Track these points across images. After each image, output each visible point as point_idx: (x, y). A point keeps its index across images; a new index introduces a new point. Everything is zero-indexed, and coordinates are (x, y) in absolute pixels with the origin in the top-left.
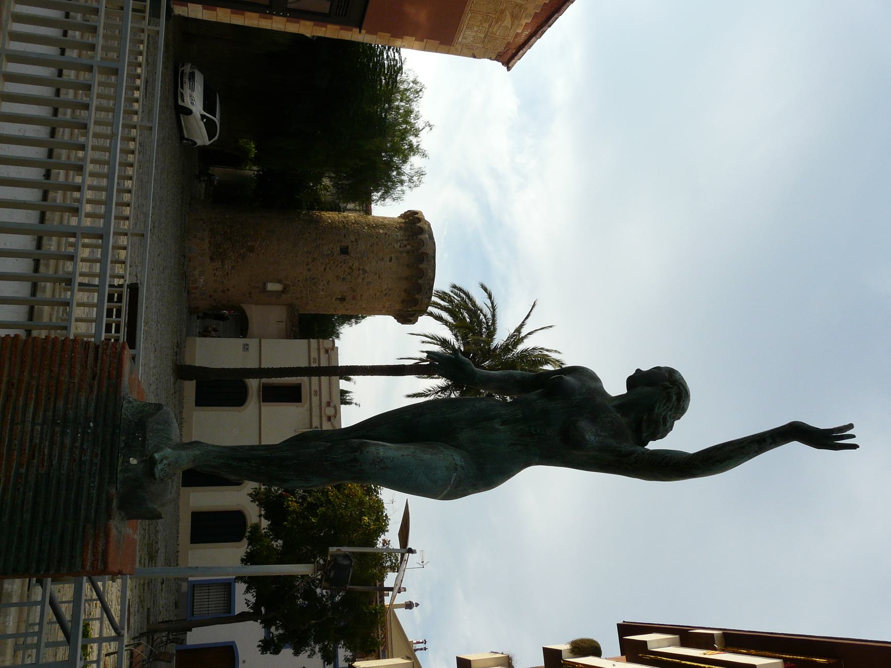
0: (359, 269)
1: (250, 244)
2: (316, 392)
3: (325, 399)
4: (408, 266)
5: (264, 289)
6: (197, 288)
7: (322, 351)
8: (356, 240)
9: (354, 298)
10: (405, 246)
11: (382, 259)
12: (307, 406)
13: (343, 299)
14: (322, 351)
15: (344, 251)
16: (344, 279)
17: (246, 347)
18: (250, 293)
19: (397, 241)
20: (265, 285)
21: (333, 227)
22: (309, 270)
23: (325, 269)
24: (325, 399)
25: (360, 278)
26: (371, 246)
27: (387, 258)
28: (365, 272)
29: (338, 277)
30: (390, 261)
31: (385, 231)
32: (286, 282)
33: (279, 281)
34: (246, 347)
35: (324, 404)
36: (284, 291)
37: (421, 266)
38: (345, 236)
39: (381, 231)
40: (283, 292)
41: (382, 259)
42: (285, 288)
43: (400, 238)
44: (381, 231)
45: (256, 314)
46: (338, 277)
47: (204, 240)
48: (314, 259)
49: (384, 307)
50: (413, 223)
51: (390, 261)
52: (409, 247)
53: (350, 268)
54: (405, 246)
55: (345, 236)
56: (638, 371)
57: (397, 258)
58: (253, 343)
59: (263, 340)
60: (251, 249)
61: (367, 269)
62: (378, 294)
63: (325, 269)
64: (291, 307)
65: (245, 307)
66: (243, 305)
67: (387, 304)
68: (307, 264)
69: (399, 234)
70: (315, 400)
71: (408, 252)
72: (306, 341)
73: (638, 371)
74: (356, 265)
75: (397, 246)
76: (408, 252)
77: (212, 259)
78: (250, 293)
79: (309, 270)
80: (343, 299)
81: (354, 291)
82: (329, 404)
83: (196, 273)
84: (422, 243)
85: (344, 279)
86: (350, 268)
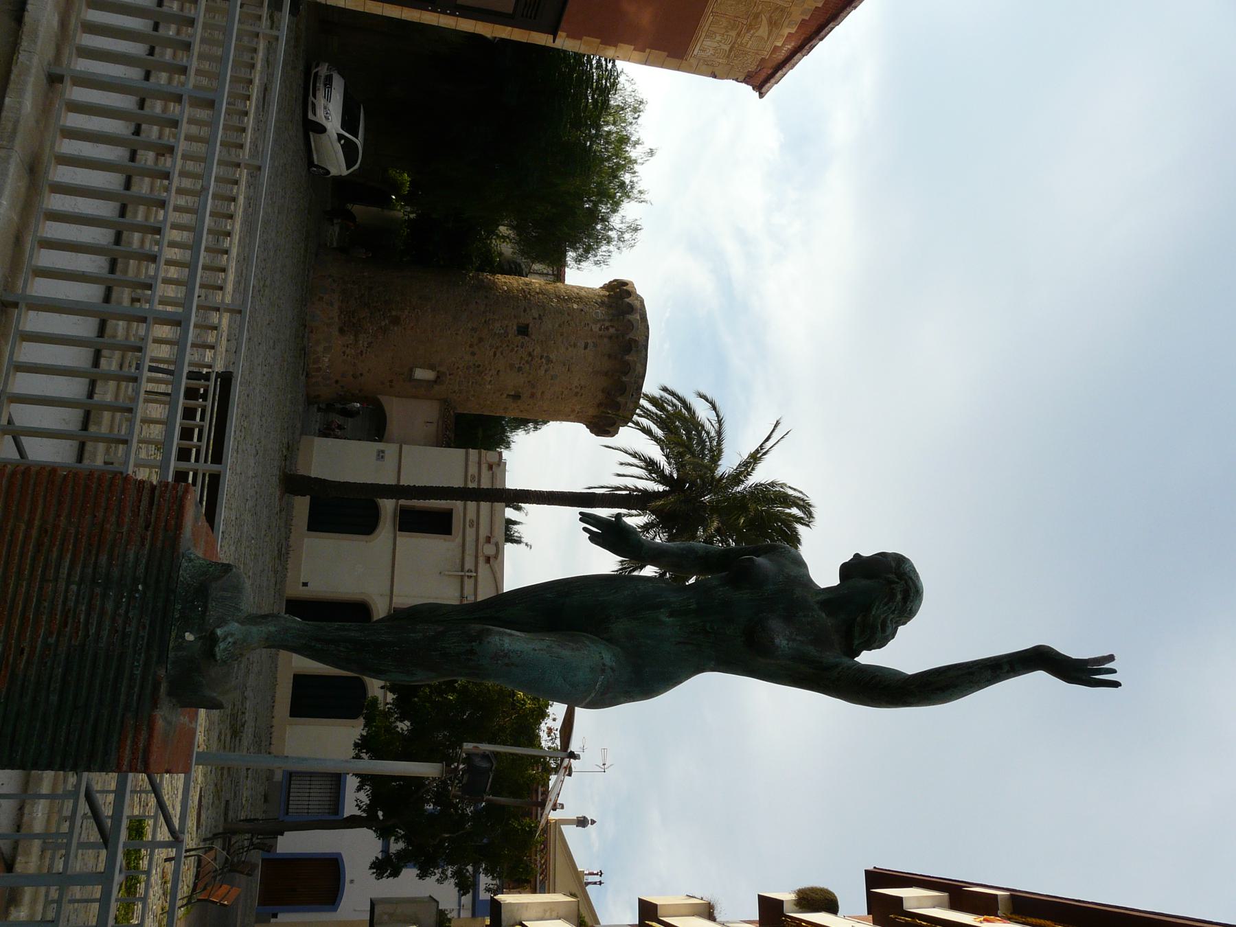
1: (394, 313)
2: (471, 522)
3: (484, 532)
4: (610, 356)
5: (410, 378)
6: (319, 369)
9: (533, 395)
10: (607, 328)
11: (575, 345)
12: (459, 540)
13: (517, 397)
15: (523, 330)
17: (381, 455)
18: (391, 381)
19: (596, 321)
20: (411, 371)
21: (509, 297)
22: (473, 354)
23: (495, 354)
24: (484, 532)
27: (581, 344)
28: (549, 361)
29: (512, 366)
30: (586, 348)
31: (581, 307)
32: (442, 369)
33: (431, 367)
34: (381, 455)
35: (482, 540)
36: (438, 380)
37: (627, 357)
38: (525, 310)
39: (575, 306)
40: (435, 382)
41: (575, 345)
42: (438, 377)
43: (600, 317)
44: (575, 306)
45: (395, 409)
46: (512, 366)
47: (332, 304)
48: (481, 340)
49: (573, 411)
50: (621, 299)
51: (586, 348)
52: (612, 330)
53: (530, 354)
54: (607, 328)
55: (525, 310)
56: (857, 556)
57: (595, 345)
58: (390, 449)
60: (396, 321)
61: (552, 356)
63: (495, 354)
64: (446, 403)
65: (384, 399)
67: (577, 408)
68: (471, 346)
69: (601, 312)
70: (470, 532)
71: (610, 338)
72: (462, 451)
73: (857, 556)
74: (538, 350)
75: (596, 328)
77: (341, 331)
78: (391, 381)
80: (517, 397)
82: (488, 540)
83: (320, 349)
84: (630, 326)
85: (520, 369)
86: (530, 354)
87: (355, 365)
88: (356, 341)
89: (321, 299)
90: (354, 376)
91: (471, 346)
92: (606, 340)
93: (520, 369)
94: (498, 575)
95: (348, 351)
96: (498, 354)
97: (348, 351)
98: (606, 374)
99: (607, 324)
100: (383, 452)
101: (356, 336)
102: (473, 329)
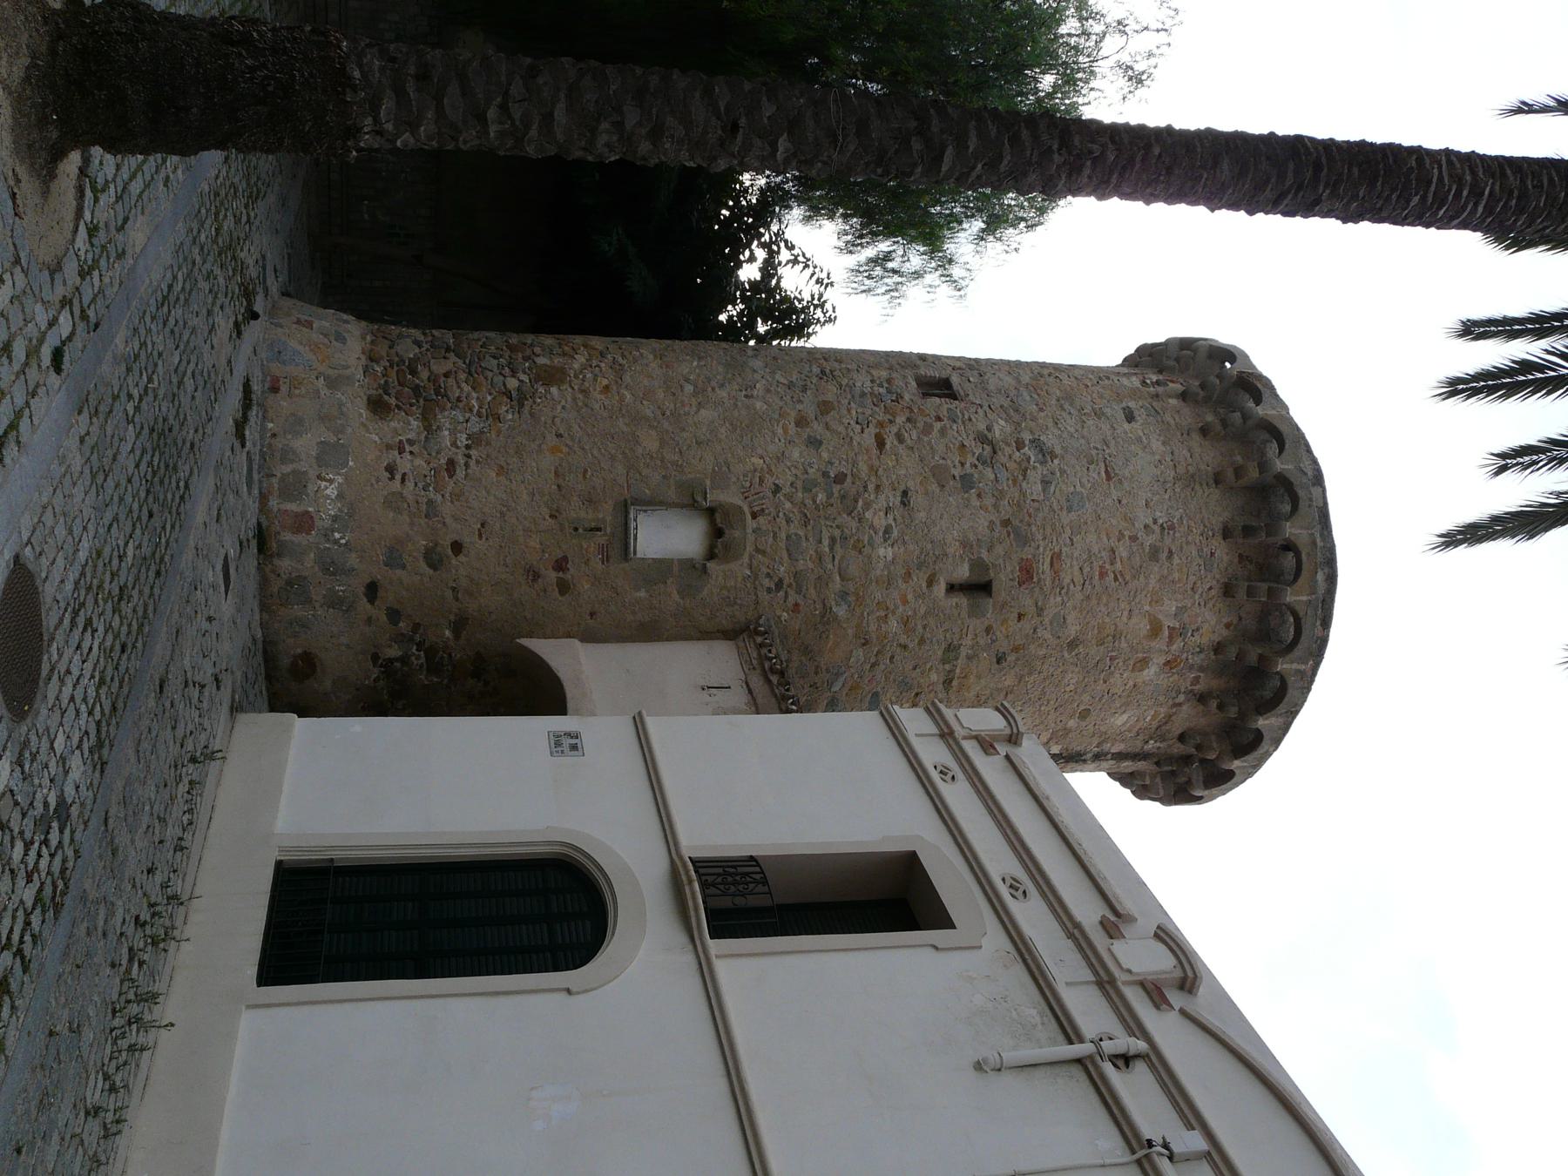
0: (1020, 445)
1: (541, 361)
4: (1204, 431)
6: (303, 523)
9: (1027, 573)
16: (967, 482)
18: (560, 565)
22: (814, 443)
23: (881, 443)
25: (1035, 476)
28: (1046, 454)
29: (940, 475)
32: (729, 497)
33: (691, 500)
40: (711, 555)
42: (717, 533)
46: (940, 475)
48: (825, 408)
49: (1155, 630)
61: (1050, 440)
62: (1122, 552)
63: (881, 443)
66: (525, 642)
74: (1001, 428)
77: (377, 406)
78: (560, 565)
80: (978, 588)
81: (1024, 540)
86: (982, 439)
87: (431, 510)
88: (430, 428)
90: (433, 559)
91: (801, 422)
93: (967, 482)
95: (405, 464)
97: (405, 464)
98: (1218, 479)
102: (790, 386)
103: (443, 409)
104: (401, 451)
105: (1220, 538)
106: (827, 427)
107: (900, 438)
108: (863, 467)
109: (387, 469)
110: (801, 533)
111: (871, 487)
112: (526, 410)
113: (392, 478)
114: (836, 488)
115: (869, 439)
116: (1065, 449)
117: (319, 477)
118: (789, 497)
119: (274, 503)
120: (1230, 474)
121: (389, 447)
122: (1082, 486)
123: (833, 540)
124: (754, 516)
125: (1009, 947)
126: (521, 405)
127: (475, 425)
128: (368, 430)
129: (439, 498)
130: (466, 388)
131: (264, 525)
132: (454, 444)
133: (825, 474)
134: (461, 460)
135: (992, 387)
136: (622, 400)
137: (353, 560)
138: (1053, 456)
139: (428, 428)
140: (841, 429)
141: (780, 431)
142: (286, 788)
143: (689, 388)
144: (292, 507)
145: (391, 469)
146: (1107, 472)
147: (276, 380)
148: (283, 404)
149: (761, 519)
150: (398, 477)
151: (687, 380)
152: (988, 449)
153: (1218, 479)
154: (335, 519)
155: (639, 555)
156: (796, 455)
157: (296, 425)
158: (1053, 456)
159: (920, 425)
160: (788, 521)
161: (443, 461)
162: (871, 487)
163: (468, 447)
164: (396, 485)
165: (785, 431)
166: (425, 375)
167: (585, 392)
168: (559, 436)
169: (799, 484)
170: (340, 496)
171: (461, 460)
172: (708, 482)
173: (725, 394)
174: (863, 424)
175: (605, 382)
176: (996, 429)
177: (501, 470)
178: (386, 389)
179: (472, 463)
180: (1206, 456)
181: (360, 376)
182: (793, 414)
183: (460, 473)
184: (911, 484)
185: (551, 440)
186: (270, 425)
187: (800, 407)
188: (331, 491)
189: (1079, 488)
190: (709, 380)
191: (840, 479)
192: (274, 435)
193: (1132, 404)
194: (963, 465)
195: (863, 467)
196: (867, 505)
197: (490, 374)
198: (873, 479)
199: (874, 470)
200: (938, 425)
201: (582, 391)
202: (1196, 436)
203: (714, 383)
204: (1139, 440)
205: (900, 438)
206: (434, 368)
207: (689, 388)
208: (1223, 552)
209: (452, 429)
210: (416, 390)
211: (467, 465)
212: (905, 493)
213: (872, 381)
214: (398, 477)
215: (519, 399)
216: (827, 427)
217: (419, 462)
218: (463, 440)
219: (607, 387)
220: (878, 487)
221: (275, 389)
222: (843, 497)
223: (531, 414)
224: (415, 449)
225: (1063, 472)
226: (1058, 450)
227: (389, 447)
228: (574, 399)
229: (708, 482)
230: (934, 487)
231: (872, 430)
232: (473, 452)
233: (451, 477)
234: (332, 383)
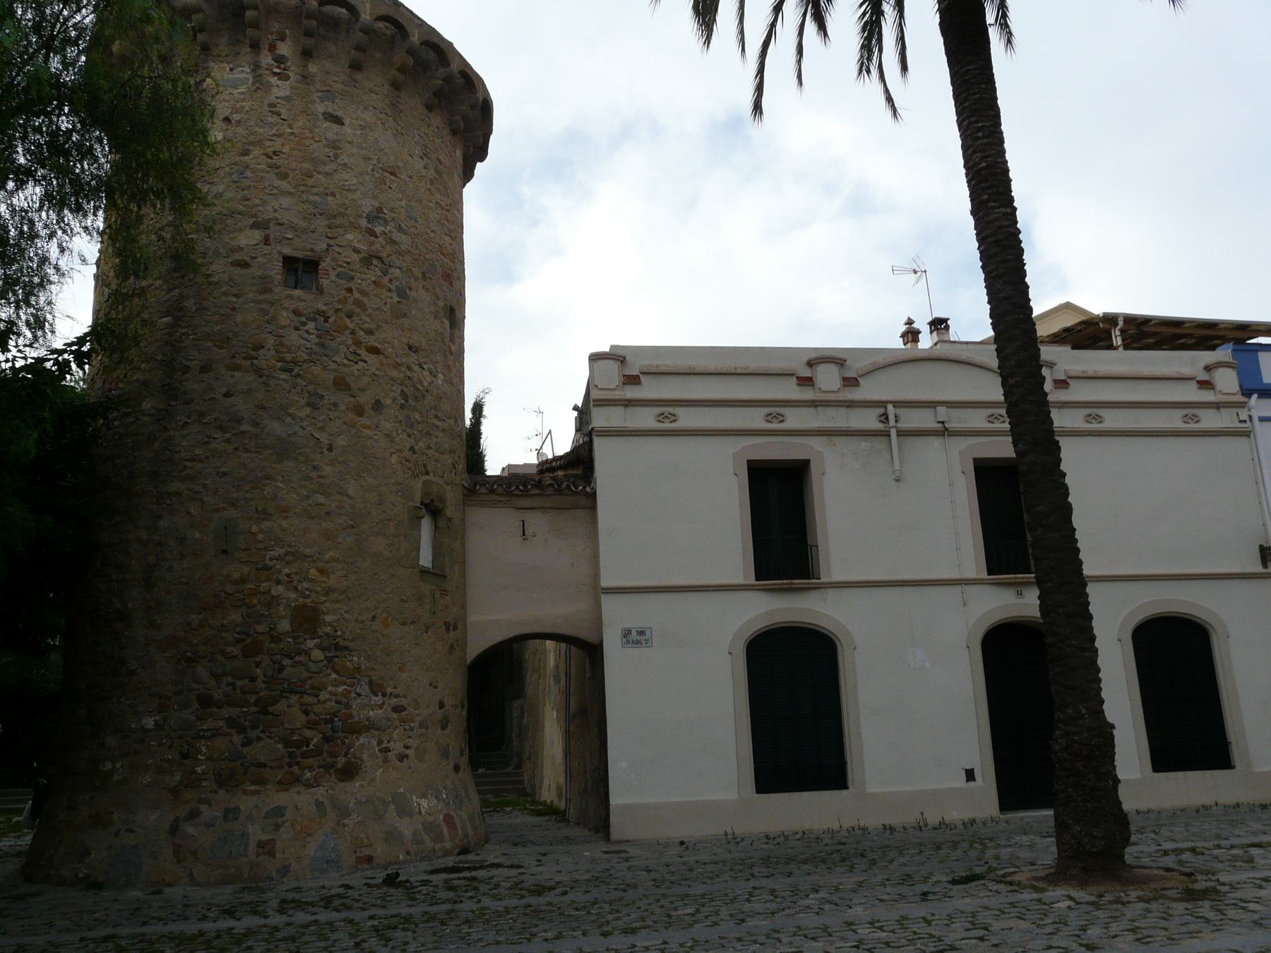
0: (372, 233)
1: (284, 625)
2: (770, 418)
3: (790, 391)
4: (356, 66)
5: (435, 575)
7: (631, 393)
8: (255, 226)
10: (280, 60)
12: (816, 443)
14: (631, 393)
15: (301, 269)
17: (635, 638)
19: (260, 84)
20: (424, 572)
23: (374, 351)
24: (790, 391)
25: (397, 236)
26: (284, 176)
27: (332, 130)
28: (376, 216)
29: (399, 314)
30: (338, 121)
34: (635, 638)
35: (808, 394)
38: (244, 265)
41: (334, 145)
43: (244, 73)
47: (278, 812)
48: (341, 384)
51: (338, 121)
53: (368, 261)
54: (280, 60)
55: (244, 265)
58: (617, 616)
59: (605, 583)
60: (307, 619)
61: (368, 205)
63: (374, 351)
68: (359, 411)
70: (795, 419)
71: (307, 54)
75: (281, 89)
76: (307, 54)
77: (349, 772)
79: (378, 406)
82: (806, 382)
83: (406, 828)
85: (402, 293)
86: (368, 261)
88: (370, 726)
89: (267, 848)
91: (359, 411)
92: (313, 68)
94: (880, 360)
95: (397, 747)
96: (372, 341)
97: (397, 747)
99: (266, 59)
100: (626, 634)
101: (357, 729)
103: (351, 716)
104: (387, 750)
105: (431, 115)
106: (362, 390)
107: (369, 332)
108: (395, 373)
109: (401, 761)
110: (435, 440)
111: (408, 373)
112: (351, 645)
113: (407, 756)
114: (411, 402)
115: (372, 359)
116: (375, 197)
117: (420, 813)
118: (417, 441)
119: (448, 845)
120: (401, 77)
121: (386, 760)
122: (400, 200)
123: (436, 416)
124: (427, 473)
125: (824, 438)
126: (346, 648)
127: (364, 689)
128: (375, 779)
129: (418, 719)
130: (323, 696)
131: (457, 850)
132: (381, 707)
133: (402, 407)
134: (394, 701)
135: (302, 224)
136: (334, 560)
137: (449, 783)
138: (380, 210)
139: (367, 728)
140: (365, 379)
141: (367, 431)
142: (694, 799)
143: (321, 499)
144: (445, 830)
145: (402, 758)
146: (391, 173)
147: (360, 860)
148: (380, 851)
149: (429, 468)
150: (407, 752)
151: (307, 497)
152: (375, 262)
153: (396, 86)
154: (437, 798)
155: (430, 566)
156: (387, 425)
157: (393, 837)
158: (380, 210)
159: (357, 310)
160: (429, 448)
161: (395, 715)
162: (408, 373)
163: (384, 695)
164: (410, 752)
165: (368, 427)
166: (308, 733)
167: (328, 591)
168: (374, 617)
169: (409, 431)
170: (424, 796)
171: (394, 701)
172: (410, 503)
173: (328, 468)
174: (356, 358)
175: (313, 571)
176: (360, 246)
177: (401, 669)
178: (328, 767)
179: (396, 691)
180: (375, 81)
181: (321, 790)
182: (351, 415)
183: (403, 701)
184: (405, 340)
185: (377, 625)
186: (401, 857)
187: (343, 407)
188: (424, 803)
189: (403, 204)
190: (308, 478)
191: (404, 395)
192: (408, 853)
193: (320, 108)
194: (390, 290)
195: (395, 373)
196: (420, 382)
197: (305, 675)
198: (403, 369)
199: (397, 366)
200: (356, 295)
201: (327, 594)
202: (358, 76)
203: (313, 474)
204: (362, 128)
205: (369, 332)
206: (298, 725)
207: (321, 499)
208: (437, 120)
209: (368, 708)
210: (327, 739)
211: (397, 696)
212: (410, 347)
213: (297, 329)
214: (407, 752)
215: (337, 648)
216: (362, 390)
217: (395, 737)
218: (378, 699)
219: (321, 571)
220: (409, 368)
221: (370, 859)
222: (416, 398)
223: (353, 640)
224: (385, 739)
225: (392, 210)
226: (377, 205)
227: (386, 760)
228: (338, 601)
229: (410, 503)
230: (406, 322)
231: (363, 353)
232: (389, 690)
233: (405, 709)
234: (344, 812)
